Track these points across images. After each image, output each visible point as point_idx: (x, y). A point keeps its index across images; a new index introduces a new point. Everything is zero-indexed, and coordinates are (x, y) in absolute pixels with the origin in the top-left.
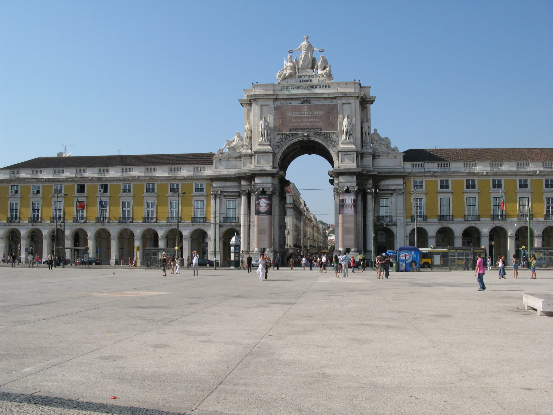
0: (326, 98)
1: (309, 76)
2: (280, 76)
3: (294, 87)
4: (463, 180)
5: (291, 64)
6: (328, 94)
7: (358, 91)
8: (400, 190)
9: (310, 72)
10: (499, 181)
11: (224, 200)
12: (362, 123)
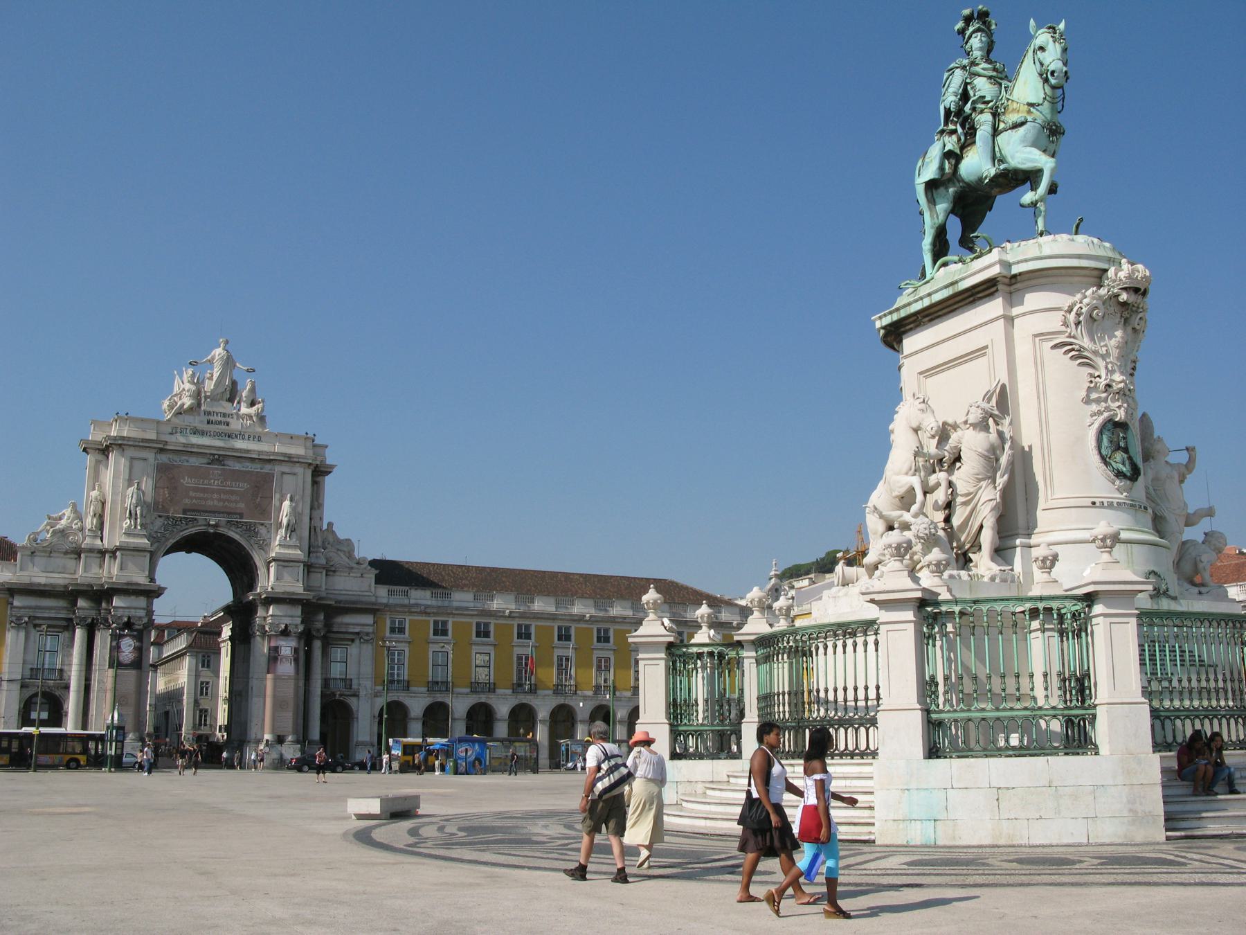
0: (252, 460)
1: (224, 415)
2: (171, 407)
3: (195, 432)
4: (471, 624)
5: (193, 388)
6: (260, 452)
7: (310, 453)
8: (368, 634)
9: (227, 407)
10: (528, 627)
11: (34, 634)
12: (312, 508)
